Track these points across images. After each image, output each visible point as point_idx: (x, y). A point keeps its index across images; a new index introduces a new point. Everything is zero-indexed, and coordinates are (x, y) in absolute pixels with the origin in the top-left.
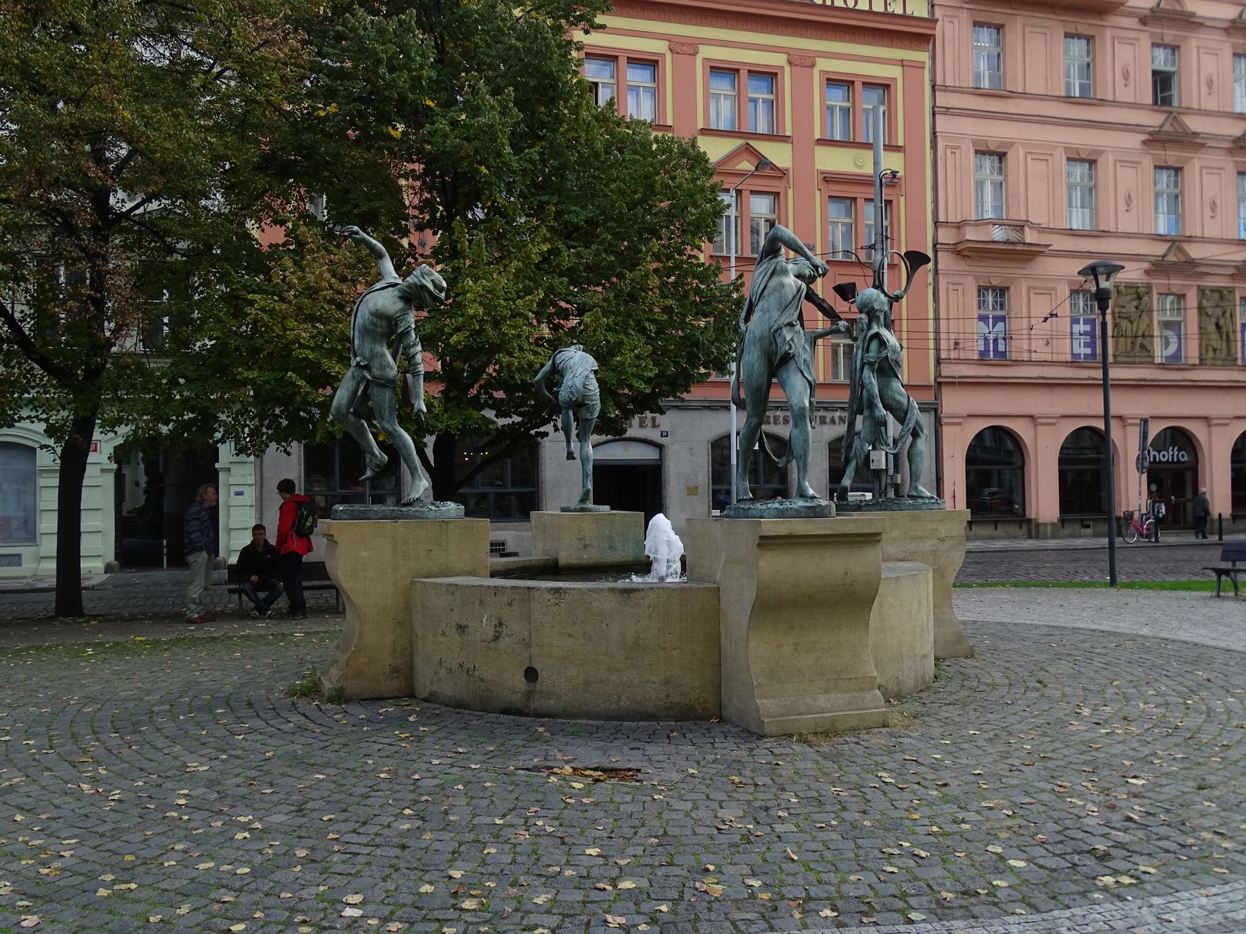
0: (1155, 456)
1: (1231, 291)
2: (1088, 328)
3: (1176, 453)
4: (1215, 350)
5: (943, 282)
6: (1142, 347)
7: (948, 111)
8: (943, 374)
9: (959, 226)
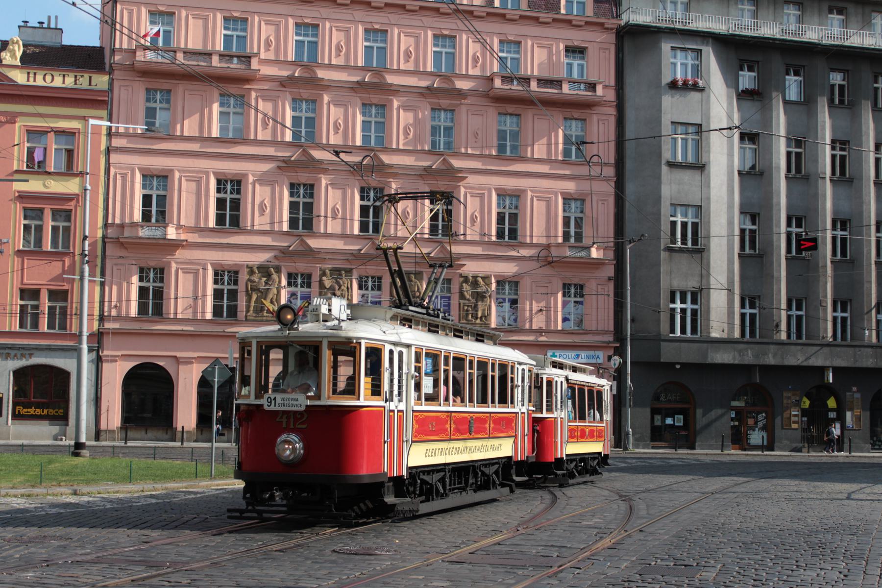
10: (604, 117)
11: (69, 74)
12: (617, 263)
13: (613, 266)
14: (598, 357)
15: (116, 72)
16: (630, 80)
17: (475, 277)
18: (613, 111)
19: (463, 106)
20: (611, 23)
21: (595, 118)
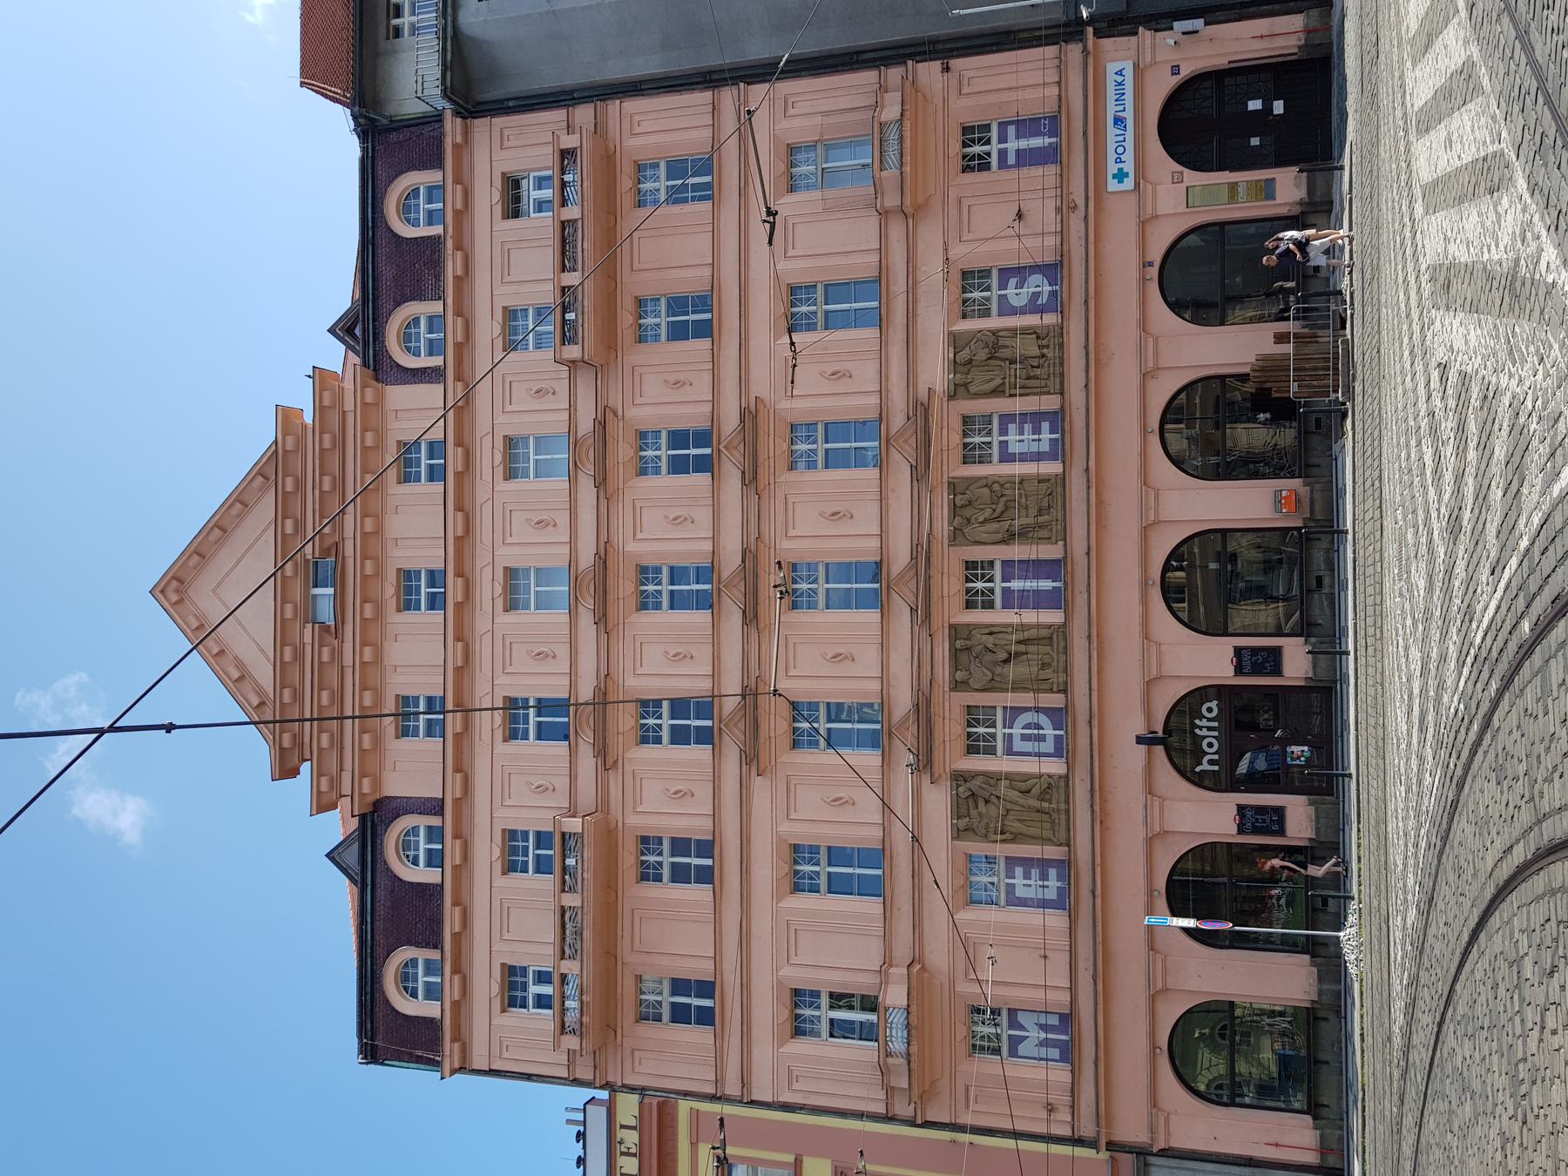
0: (1211, 762)
1: (955, 631)
2: (1019, 871)
4: (1044, 666)
5: (968, 1119)
7: (745, 1083)
8: (1093, 1134)
9: (890, 1091)
10: (626, 126)
11: (619, 1165)
12: (912, 56)
13: (920, 65)
14: (1120, 73)
15: (610, 1079)
16: (549, 80)
17: (955, 365)
18: (614, 106)
20: (452, 127)
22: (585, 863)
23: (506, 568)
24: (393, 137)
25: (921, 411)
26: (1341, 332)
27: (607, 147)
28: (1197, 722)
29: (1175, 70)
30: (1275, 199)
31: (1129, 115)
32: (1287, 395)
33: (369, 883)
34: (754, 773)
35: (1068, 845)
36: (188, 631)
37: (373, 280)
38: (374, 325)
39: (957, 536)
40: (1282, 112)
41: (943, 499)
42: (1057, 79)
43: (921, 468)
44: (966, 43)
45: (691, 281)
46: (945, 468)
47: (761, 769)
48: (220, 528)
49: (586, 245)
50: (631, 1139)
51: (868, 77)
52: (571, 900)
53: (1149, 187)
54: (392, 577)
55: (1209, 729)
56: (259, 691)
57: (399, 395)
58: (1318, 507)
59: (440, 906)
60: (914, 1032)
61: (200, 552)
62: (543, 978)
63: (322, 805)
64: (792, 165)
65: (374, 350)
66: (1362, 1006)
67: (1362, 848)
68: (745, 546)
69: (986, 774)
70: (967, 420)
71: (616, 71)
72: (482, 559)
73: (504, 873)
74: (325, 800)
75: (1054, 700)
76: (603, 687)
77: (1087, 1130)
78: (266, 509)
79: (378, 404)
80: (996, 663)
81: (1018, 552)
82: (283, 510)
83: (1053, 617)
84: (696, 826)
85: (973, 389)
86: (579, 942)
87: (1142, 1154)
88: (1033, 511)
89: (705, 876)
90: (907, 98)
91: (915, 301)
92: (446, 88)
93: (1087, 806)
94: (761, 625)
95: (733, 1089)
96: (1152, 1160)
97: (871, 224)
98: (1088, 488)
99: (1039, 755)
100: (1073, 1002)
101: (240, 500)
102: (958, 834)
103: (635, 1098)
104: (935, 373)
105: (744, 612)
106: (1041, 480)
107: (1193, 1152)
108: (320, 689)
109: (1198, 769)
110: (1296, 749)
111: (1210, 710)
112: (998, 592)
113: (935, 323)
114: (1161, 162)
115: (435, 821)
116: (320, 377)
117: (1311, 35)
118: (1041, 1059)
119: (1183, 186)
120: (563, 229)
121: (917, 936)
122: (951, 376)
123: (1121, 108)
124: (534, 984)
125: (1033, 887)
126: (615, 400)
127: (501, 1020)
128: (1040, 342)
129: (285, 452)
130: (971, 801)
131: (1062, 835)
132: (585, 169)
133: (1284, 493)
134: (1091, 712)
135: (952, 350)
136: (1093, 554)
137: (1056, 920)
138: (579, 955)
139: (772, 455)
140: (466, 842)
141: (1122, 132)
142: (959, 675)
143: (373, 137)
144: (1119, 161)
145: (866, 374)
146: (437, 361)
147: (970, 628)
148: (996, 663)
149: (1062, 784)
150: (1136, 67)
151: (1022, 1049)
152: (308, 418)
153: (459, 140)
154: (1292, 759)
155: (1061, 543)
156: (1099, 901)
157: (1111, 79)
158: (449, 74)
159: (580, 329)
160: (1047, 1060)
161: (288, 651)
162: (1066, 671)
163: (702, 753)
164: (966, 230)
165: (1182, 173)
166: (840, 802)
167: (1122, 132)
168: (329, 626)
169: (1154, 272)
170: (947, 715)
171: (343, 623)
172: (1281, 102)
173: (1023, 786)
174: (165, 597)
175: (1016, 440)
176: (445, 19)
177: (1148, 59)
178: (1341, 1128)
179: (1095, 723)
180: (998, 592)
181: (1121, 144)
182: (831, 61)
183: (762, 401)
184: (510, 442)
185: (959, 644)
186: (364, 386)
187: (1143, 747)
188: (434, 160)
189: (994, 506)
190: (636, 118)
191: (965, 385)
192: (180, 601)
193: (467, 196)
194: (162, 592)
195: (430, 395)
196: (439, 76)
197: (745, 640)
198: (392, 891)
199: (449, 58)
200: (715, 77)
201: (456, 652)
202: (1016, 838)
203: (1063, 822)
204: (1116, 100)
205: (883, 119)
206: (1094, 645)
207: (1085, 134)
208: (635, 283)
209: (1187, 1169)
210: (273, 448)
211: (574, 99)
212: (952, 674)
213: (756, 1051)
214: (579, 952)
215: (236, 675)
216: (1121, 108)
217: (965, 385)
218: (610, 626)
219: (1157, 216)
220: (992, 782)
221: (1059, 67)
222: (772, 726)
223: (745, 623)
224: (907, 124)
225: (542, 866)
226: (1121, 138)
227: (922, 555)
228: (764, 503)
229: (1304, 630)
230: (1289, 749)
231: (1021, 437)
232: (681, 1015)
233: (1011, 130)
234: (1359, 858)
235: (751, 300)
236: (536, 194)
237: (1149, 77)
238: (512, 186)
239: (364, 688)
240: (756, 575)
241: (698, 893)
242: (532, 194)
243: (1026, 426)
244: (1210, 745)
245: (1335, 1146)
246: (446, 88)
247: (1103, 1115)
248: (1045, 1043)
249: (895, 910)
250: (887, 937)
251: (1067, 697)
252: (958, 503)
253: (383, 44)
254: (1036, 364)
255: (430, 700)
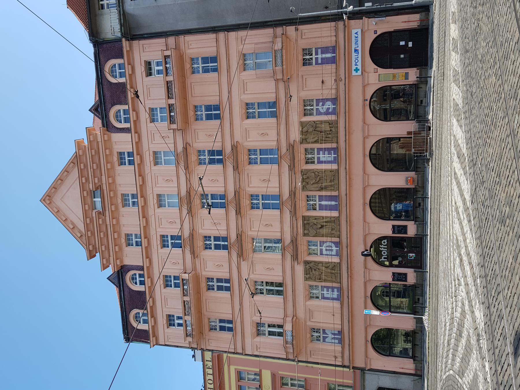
0: (384, 258)
1: (304, 218)
2: (325, 289)
3: (382, 246)
4: (332, 229)
6: (332, 269)
7: (243, 349)
9: (287, 353)
10: (186, 45)
11: (206, 371)
13: (288, 27)
14: (356, 33)
15: (202, 347)
17: (302, 133)
18: (181, 38)
19: (194, 145)
20: (125, 44)
21: (189, 51)
22: (190, 288)
23: (157, 195)
24: (105, 46)
25: (291, 147)
26: (429, 132)
27: (180, 53)
28: (380, 246)
29: (375, 32)
30: (408, 79)
31: (359, 48)
32: (411, 153)
33: (122, 290)
34: (242, 260)
35: (340, 283)
36: (55, 213)
37: (103, 97)
38: (105, 112)
39: (304, 188)
40: (411, 46)
41: (299, 178)
42: (335, 35)
43: (292, 167)
44: (303, 20)
45: (213, 100)
46: (300, 166)
47: (244, 258)
48: (60, 180)
49: (176, 90)
50: (210, 364)
51: (269, 31)
52: (186, 299)
53: (366, 74)
54: (120, 196)
55: (384, 248)
56: (80, 232)
57: (116, 137)
58: (420, 182)
59: (145, 298)
60: (294, 338)
61: (55, 187)
62: (179, 318)
63: (104, 267)
64: (245, 60)
65: (106, 121)
66: (429, 340)
67: (430, 295)
68: (235, 190)
69: (315, 262)
70: (306, 150)
71: (181, 26)
72: (149, 191)
73: (164, 288)
74: (105, 266)
75: (337, 240)
76: (192, 233)
77: (347, 363)
78: (75, 173)
79: (109, 140)
80: (317, 229)
81: (324, 193)
82: (81, 175)
83: (335, 214)
84: (225, 275)
85: (308, 141)
86: (190, 311)
87: (363, 370)
88: (328, 181)
89: (228, 289)
90: (284, 41)
91: (288, 110)
92: (122, 33)
93: (346, 272)
94: (242, 215)
95: (240, 350)
96: (365, 372)
97: (273, 83)
98: (346, 175)
99: (332, 255)
100: (342, 328)
101: (66, 171)
102: (306, 279)
103: (210, 353)
104: (295, 135)
105: (236, 211)
106: (331, 171)
107: (378, 370)
108: (100, 232)
109: (380, 260)
110: (411, 255)
111: (384, 242)
112: (317, 205)
113: (295, 118)
114: (371, 66)
115: (142, 272)
116: (89, 131)
117: (422, 22)
118: (332, 343)
119: (378, 74)
120: (167, 84)
121: (294, 309)
122: (301, 136)
123: (357, 46)
124: (177, 320)
125: (330, 294)
126: (189, 140)
127: (167, 330)
128: (331, 126)
129: (79, 155)
130: (310, 270)
131: (339, 280)
132: (173, 63)
133: (409, 178)
134: (347, 245)
135: (301, 127)
136: (348, 195)
137: (337, 304)
138: (190, 314)
139: (243, 160)
140: (152, 279)
141: (358, 55)
142: (306, 232)
143: (98, 46)
144: (356, 65)
145: (273, 135)
146: (127, 125)
147: (309, 217)
148: (317, 229)
149: (338, 265)
150: (362, 31)
151: (327, 340)
152: (86, 142)
153: (128, 49)
154: (410, 257)
155: (338, 191)
156: (350, 300)
157: (354, 35)
158: (123, 28)
159: (176, 118)
160: (335, 343)
161: (88, 220)
162: (339, 231)
163: (225, 253)
164: (305, 86)
165: (377, 69)
166: (269, 269)
167: (358, 55)
168: (101, 212)
169: (368, 103)
170: (302, 244)
171: (105, 211)
172: (411, 43)
173: (327, 265)
174: (45, 202)
175: (324, 157)
176: (120, 8)
177: (366, 28)
178: (422, 364)
179: (349, 248)
180: (317, 205)
181: (357, 59)
182: (256, 25)
183: (239, 142)
184: (155, 153)
185: (305, 222)
186: (104, 134)
187: (363, 257)
188: (120, 55)
189: (316, 179)
190: (190, 43)
191: (306, 139)
192: (50, 203)
193: (155, 322)
194: (44, 200)
195: (127, 137)
196: (120, 28)
197: (237, 219)
198: (130, 293)
199: (122, 22)
200: (216, 29)
201: (143, 222)
202: (325, 281)
203: (339, 276)
204: (355, 43)
205: (276, 49)
206: (348, 224)
207: (345, 55)
208: (193, 101)
209: (375, 374)
210: (75, 154)
211: (167, 35)
212: (303, 231)
213: (246, 340)
214: (190, 313)
215: (72, 227)
216: (357, 46)
217: (306, 139)
218: (193, 214)
219: (369, 84)
220: (317, 264)
221: (335, 30)
222: (247, 246)
223: (236, 214)
224: (284, 51)
225: (177, 286)
226: (357, 57)
227: (293, 194)
228: (241, 176)
229: (415, 220)
230: (409, 255)
231: (325, 156)
232: (222, 329)
233: (319, 51)
234: (429, 298)
235: (233, 108)
236: (157, 68)
237: (366, 34)
238: (148, 64)
239: (114, 232)
240: (239, 200)
241: (225, 294)
242: (155, 68)
243: (326, 152)
244: (384, 253)
245: (419, 369)
246: (122, 33)
247: (351, 358)
248: (334, 338)
249: (287, 301)
250: (285, 309)
251: (340, 239)
252: (304, 178)
253: (98, 12)
254: (329, 133)
255: (136, 235)
